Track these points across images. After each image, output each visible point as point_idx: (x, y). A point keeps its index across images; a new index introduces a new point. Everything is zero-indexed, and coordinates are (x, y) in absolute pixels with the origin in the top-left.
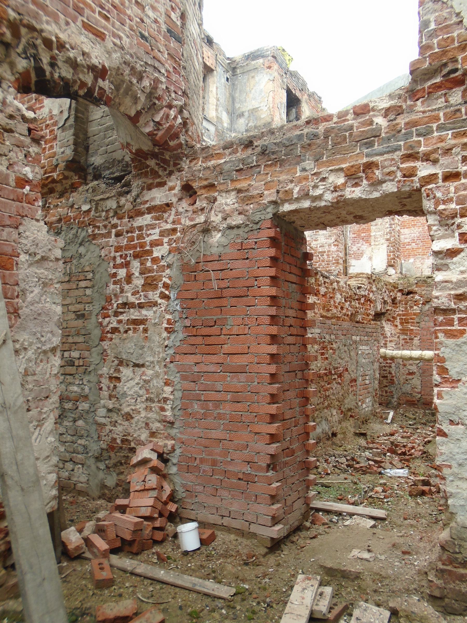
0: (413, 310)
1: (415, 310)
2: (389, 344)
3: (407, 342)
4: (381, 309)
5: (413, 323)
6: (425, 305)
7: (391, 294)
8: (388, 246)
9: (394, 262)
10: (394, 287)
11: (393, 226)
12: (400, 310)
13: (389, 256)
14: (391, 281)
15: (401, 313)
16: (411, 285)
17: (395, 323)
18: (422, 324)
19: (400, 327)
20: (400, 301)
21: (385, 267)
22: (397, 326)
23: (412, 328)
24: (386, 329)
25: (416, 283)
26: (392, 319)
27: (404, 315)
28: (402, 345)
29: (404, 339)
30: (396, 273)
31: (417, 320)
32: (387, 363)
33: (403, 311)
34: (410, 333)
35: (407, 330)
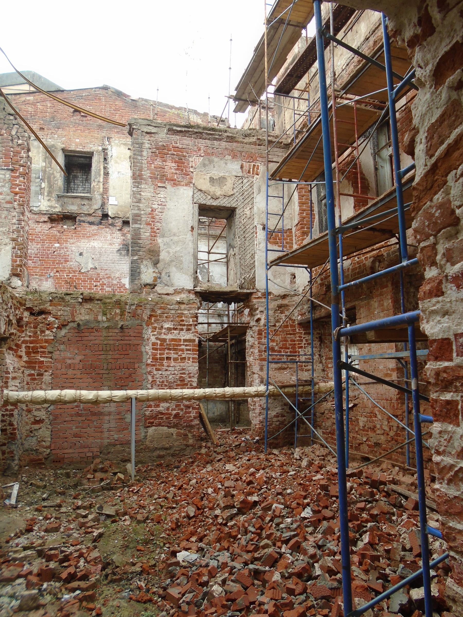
0: (44, 336)
1: (48, 335)
2: (11, 383)
3: (35, 379)
4: (5, 331)
5: (43, 352)
6: (61, 329)
7: (17, 312)
8: (14, 248)
9: (21, 271)
10: (21, 304)
11: (23, 223)
12: (27, 335)
13: (14, 261)
14: (17, 295)
15: (27, 339)
16: (44, 302)
17: (19, 353)
18: (56, 355)
19: (25, 358)
20: (28, 323)
21: (7, 276)
22: (21, 357)
23: (42, 359)
24: (8, 361)
25: (51, 301)
26: (14, 348)
27: (31, 342)
28: (28, 384)
29: (29, 375)
30: (22, 285)
31: (49, 349)
32: (7, 410)
33: (30, 336)
34: (39, 367)
35: (35, 363)
